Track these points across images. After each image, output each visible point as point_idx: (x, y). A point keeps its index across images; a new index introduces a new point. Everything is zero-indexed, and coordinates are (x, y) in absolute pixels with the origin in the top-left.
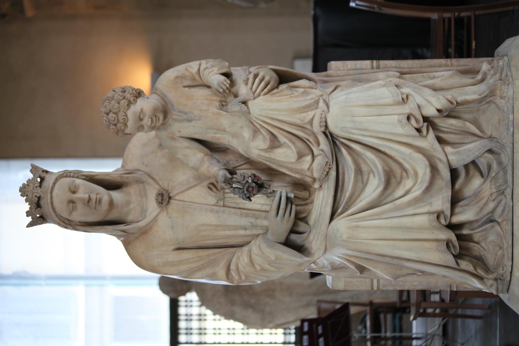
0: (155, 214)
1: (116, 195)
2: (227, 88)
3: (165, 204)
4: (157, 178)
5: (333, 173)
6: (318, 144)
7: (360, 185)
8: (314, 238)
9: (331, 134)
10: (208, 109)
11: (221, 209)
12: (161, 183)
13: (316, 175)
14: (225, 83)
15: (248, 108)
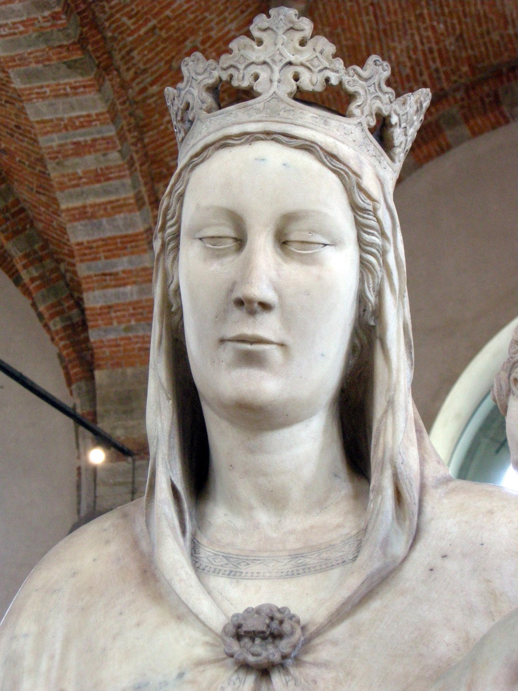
0: (204, 607)
1: (308, 444)
3: (235, 647)
4: (364, 615)
12: (340, 631)
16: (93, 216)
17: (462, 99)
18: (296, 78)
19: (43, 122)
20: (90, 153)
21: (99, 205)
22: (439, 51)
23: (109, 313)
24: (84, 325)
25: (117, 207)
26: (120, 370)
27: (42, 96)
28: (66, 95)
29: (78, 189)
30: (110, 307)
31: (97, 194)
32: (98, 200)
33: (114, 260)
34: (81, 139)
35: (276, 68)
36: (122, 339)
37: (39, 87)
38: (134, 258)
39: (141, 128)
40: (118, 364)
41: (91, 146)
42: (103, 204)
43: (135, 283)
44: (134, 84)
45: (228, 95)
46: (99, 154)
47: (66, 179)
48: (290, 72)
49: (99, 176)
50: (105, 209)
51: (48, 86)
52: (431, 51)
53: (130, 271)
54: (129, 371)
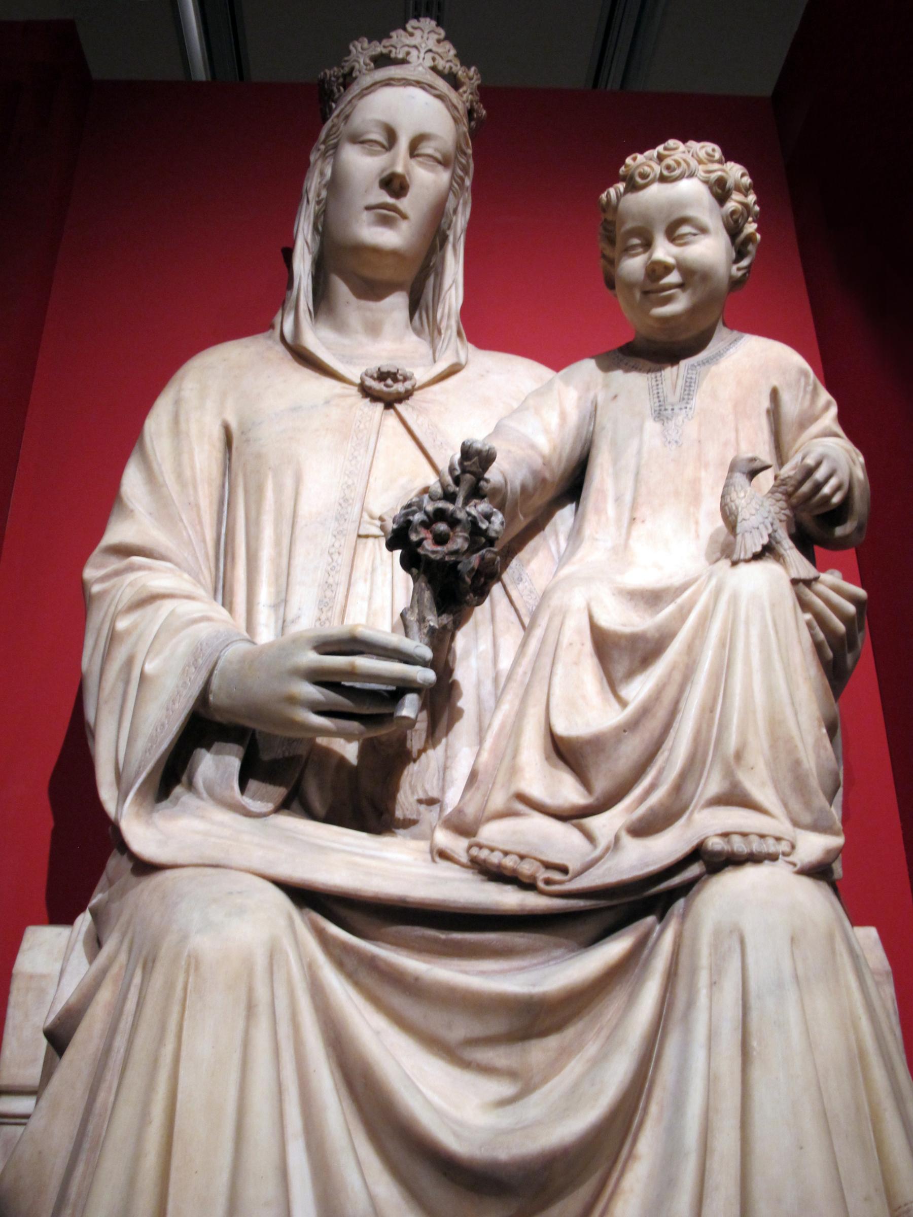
2: (819, 486)
5: (509, 899)
6: (643, 829)
7: (459, 1029)
8: (222, 824)
9: (686, 889)
10: (706, 465)
11: (351, 529)
13: (490, 832)
14: (833, 482)
15: (757, 557)
18: (434, 59)
35: (423, 51)
45: (382, 61)
48: (430, 55)
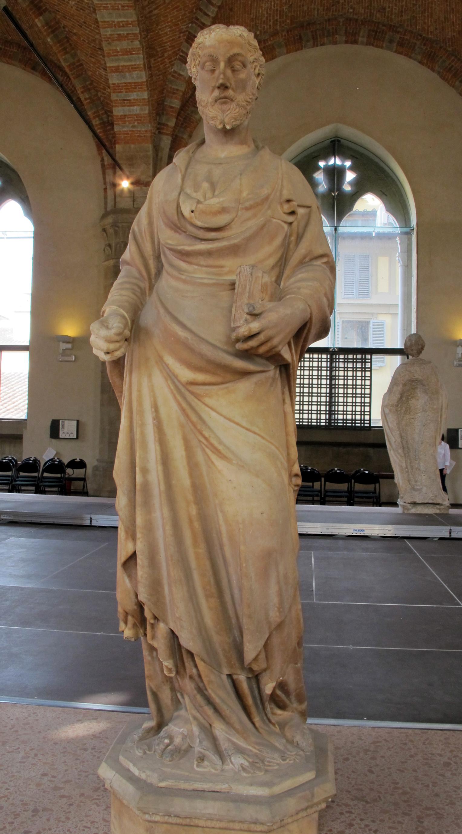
16: (122, 71)
17: (285, 36)
19: (104, 22)
20: (125, 40)
21: (126, 66)
22: (280, 11)
23: (125, 118)
24: (112, 124)
25: (134, 68)
26: (128, 145)
27: (106, 8)
28: (118, 9)
29: (116, 57)
30: (125, 116)
31: (126, 61)
32: (126, 64)
33: (130, 93)
34: (122, 33)
36: (130, 131)
37: (105, 4)
38: (139, 93)
39: (148, 31)
40: (128, 143)
41: (126, 37)
42: (128, 66)
43: (138, 105)
44: (147, 8)
46: (129, 41)
47: (111, 52)
49: (126, 52)
50: (128, 69)
51: (110, 4)
52: (277, 10)
53: (137, 100)
54: (132, 146)
